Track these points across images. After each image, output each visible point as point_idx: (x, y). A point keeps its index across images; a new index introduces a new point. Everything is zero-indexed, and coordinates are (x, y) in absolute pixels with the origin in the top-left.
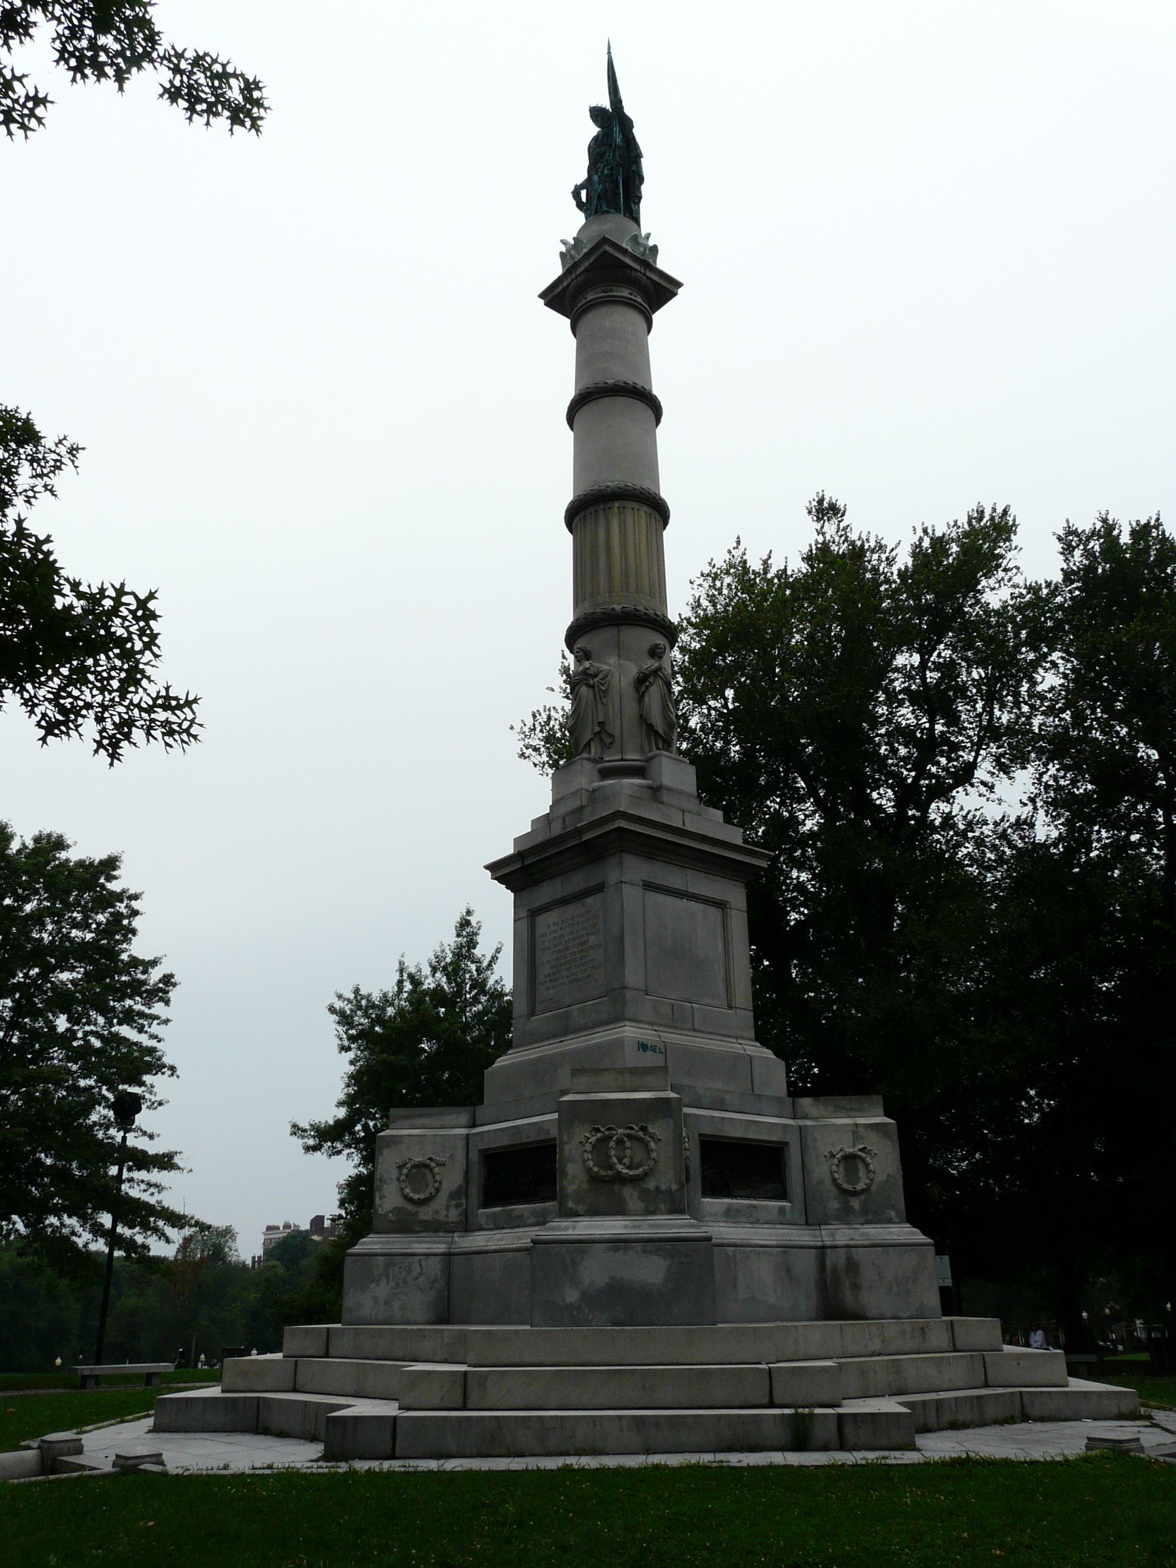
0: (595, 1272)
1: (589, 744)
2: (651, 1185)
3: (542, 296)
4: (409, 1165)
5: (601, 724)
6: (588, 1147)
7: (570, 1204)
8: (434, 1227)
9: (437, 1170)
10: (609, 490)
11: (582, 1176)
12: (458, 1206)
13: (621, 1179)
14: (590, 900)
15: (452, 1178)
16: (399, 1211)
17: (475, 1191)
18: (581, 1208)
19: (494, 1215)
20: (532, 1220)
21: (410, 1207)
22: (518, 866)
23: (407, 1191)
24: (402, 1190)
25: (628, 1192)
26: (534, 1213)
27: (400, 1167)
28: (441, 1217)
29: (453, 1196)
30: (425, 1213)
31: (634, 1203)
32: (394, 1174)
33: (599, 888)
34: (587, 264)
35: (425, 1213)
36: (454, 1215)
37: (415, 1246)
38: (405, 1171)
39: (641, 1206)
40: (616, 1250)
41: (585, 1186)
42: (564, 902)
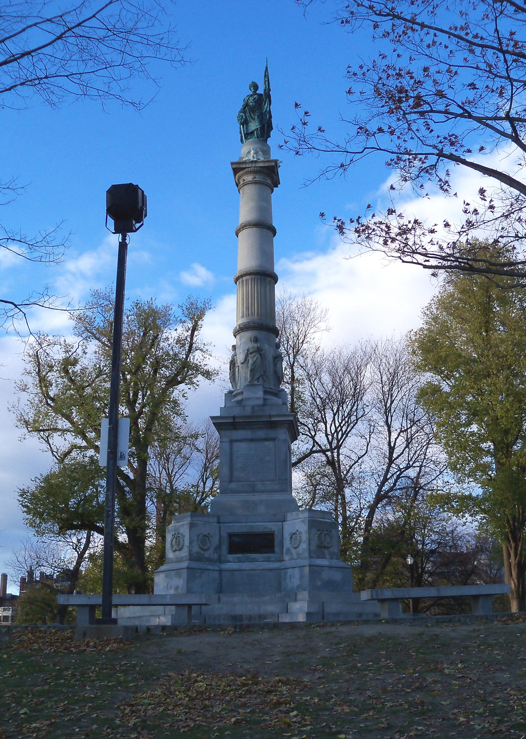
0: (326, 575)
1: (258, 378)
2: (331, 550)
3: (232, 164)
5: (264, 372)
7: (312, 554)
10: (268, 273)
12: (217, 553)
13: (325, 547)
14: (267, 443)
15: (215, 541)
16: (197, 553)
18: (314, 556)
20: (261, 560)
21: (202, 552)
22: (231, 421)
25: (326, 551)
27: (198, 536)
31: (328, 556)
32: (196, 538)
33: (274, 439)
34: (262, 165)
35: (207, 554)
36: (216, 556)
39: (329, 557)
42: (252, 440)
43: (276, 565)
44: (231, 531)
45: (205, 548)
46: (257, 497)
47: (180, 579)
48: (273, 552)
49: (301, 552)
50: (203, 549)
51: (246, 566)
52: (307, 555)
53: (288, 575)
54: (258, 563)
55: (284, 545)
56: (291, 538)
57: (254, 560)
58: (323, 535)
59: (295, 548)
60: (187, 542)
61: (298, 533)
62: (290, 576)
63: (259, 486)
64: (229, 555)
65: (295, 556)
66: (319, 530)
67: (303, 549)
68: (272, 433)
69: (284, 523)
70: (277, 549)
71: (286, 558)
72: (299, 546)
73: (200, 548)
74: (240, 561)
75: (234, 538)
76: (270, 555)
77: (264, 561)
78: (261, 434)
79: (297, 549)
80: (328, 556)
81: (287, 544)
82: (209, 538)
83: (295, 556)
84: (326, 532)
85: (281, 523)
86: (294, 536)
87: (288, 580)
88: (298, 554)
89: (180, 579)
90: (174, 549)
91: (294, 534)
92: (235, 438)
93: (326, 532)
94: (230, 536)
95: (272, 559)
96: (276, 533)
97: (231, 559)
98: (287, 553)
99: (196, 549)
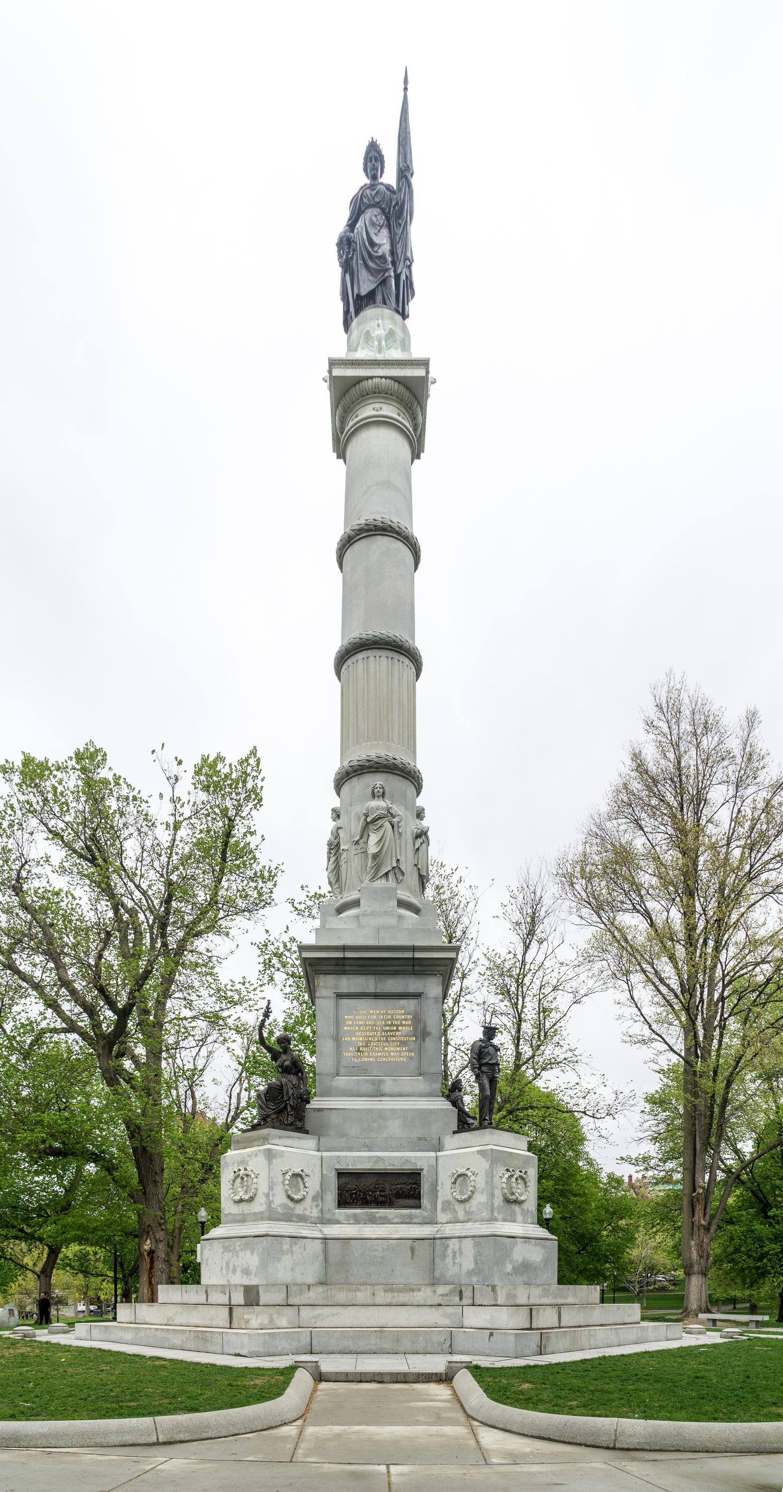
2: (525, 1206)
4: (290, 1173)
6: (504, 1180)
8: (302, 1219)
9: (306, 1179)
11: (501, 1198)
14: (403, 1002)
15: (313, 1184)
16: (285, 1206)
17: (331, 1196)
19: (355, 1214)
23: (290, 1193)
24: (286, 1191)
25: (517, 1208)
26: (402, 1216)
28: (307, 1213)
29: (314, 1199)
30: (299, 1209)
31: (519, 1217)
32: (281, 1179)
33: (417, 996)
35: (299, 1209)
36: (315, 1213)
37: (302, 1231)
38: (288, 1177)
40: (526, 1242)
41: (502, 1204)
42: (376, 996)
43: (425, 1231)
44: (342, 1166)
45: (296, 1197)
46: (387, 1104)
47: (252, 1253)
48: (419, 1207)
49: (474, 1209)
50: (292, 1199)
51: (369, 1231)
52: (485, 1214)
53: (450, 1251)
54: (388, 1227)
55: (439, 1194)
56: (454, 1183)
57: (385, 1221)
58: (514, 1180)
59: (461, 1202)
60: (263, 1188)
61: (470, 1174)
62: (454, 1253)
63: (389, 1084)
64: (337, 1210)
65: (461, 1215)
66: (508, 1170)
67: (479, 1203)
68: (413, 985)
69: (439, 1154)
70: (425, 1201)
71: (442, 1217)
72: (470, 1197)
73: (289, 1197)
74: (357, 1221)
75: (344, 1180)
76: (413, 1211)
77: (402, 1223)
78: (393, 984)
79: (467, 1205)
80: (519, 1217)
81: (446, 1191)
82: (303, 1179)
83: (461, 1215)
84: (518, 1173)
85: (433, 1154)
86: (462, 1178)
87: (449, 1260)
88: (467, 1213)
89: (252, 1253)
90: (237, 1198)
91: (460, 1176)
92: (344, 990)
93: (518, 1173)
94: (340, 1174)
95: (415, 1220)
96: (425, 1172)
97: (342, 1218)
98: (444, 1210)
99: (280, 1199)
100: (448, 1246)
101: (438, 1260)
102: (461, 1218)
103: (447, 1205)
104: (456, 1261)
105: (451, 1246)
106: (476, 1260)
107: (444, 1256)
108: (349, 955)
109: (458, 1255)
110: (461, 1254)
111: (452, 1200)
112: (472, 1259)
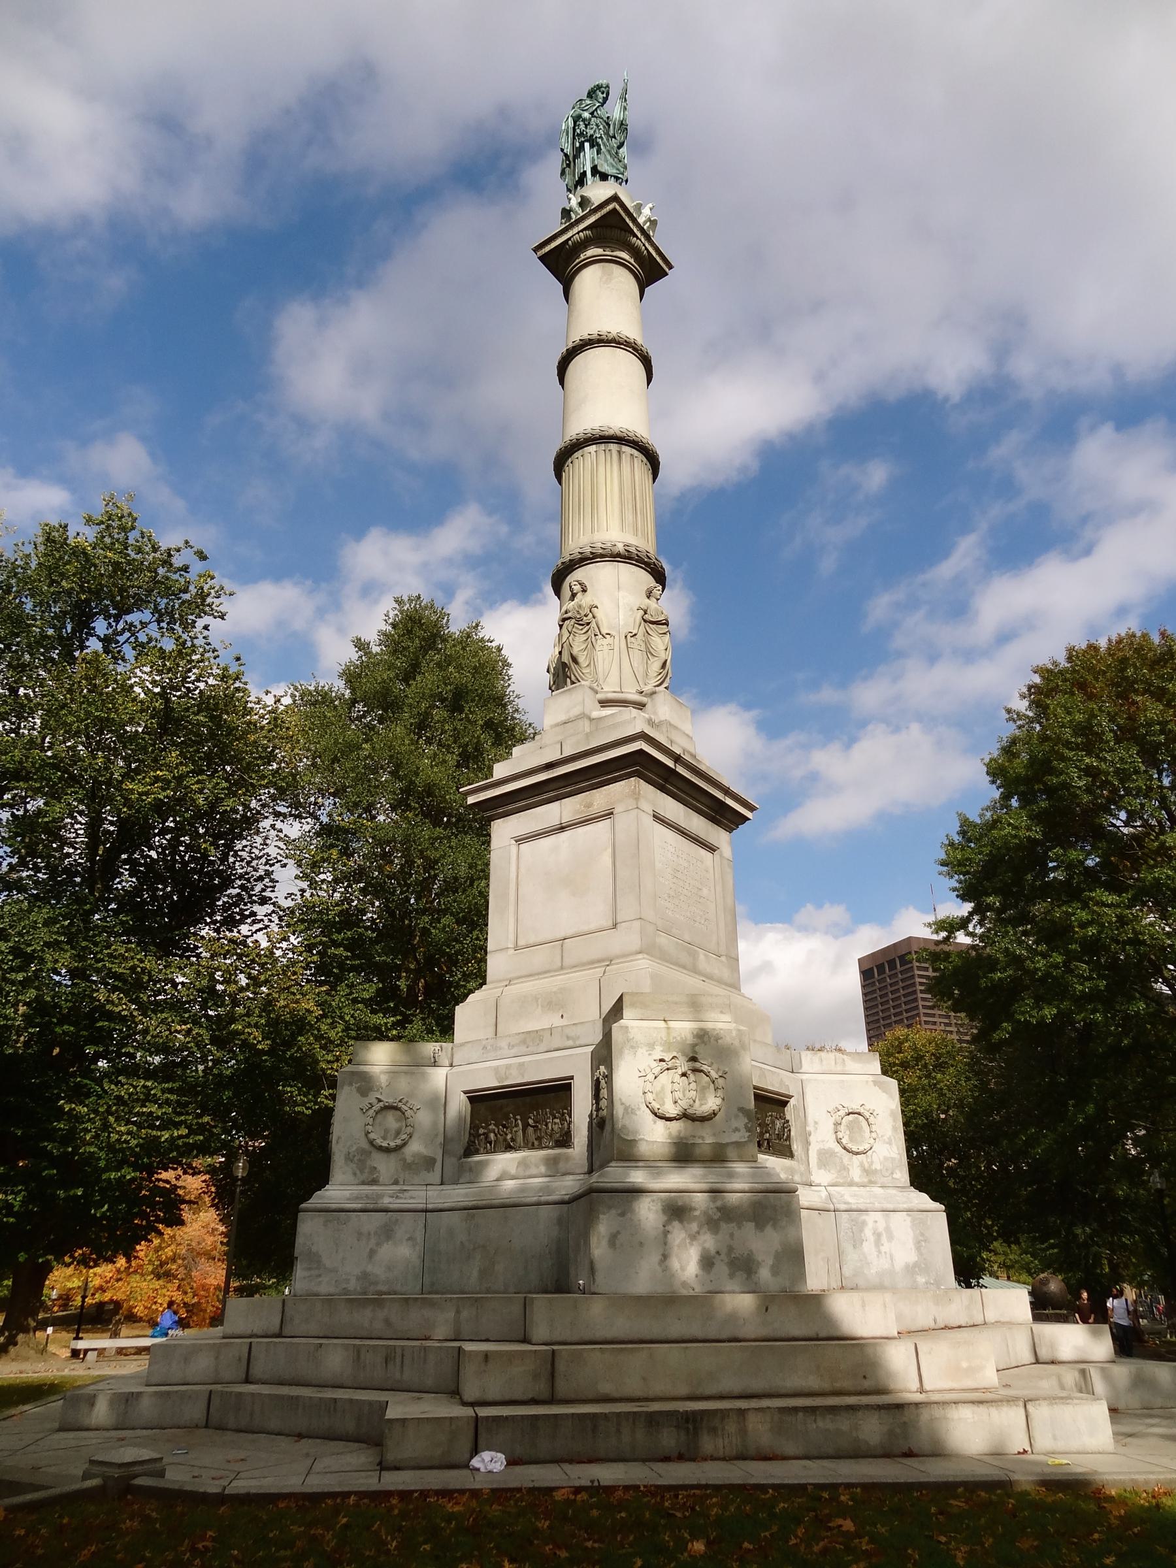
49: (877, 1166)
53: (868, 1232)
55: (812, 1139)
62: (878, 1236)
70: (796, 1147)
83: (856, 1174)
87: (868, 1247)
88: (867, 1172)
100: (864, 1223)
101: (847, 1247)
102: (857, 1179)
103: (826, 1159)
104: (883, 1249)
105: (870, 1225)
106: (918, 1248)
107: (857, 1242)
108: (681, 770)
109: (884, 1239)
110: (891, 1238)
111: (839, 1149)
112: (911, 1244)
